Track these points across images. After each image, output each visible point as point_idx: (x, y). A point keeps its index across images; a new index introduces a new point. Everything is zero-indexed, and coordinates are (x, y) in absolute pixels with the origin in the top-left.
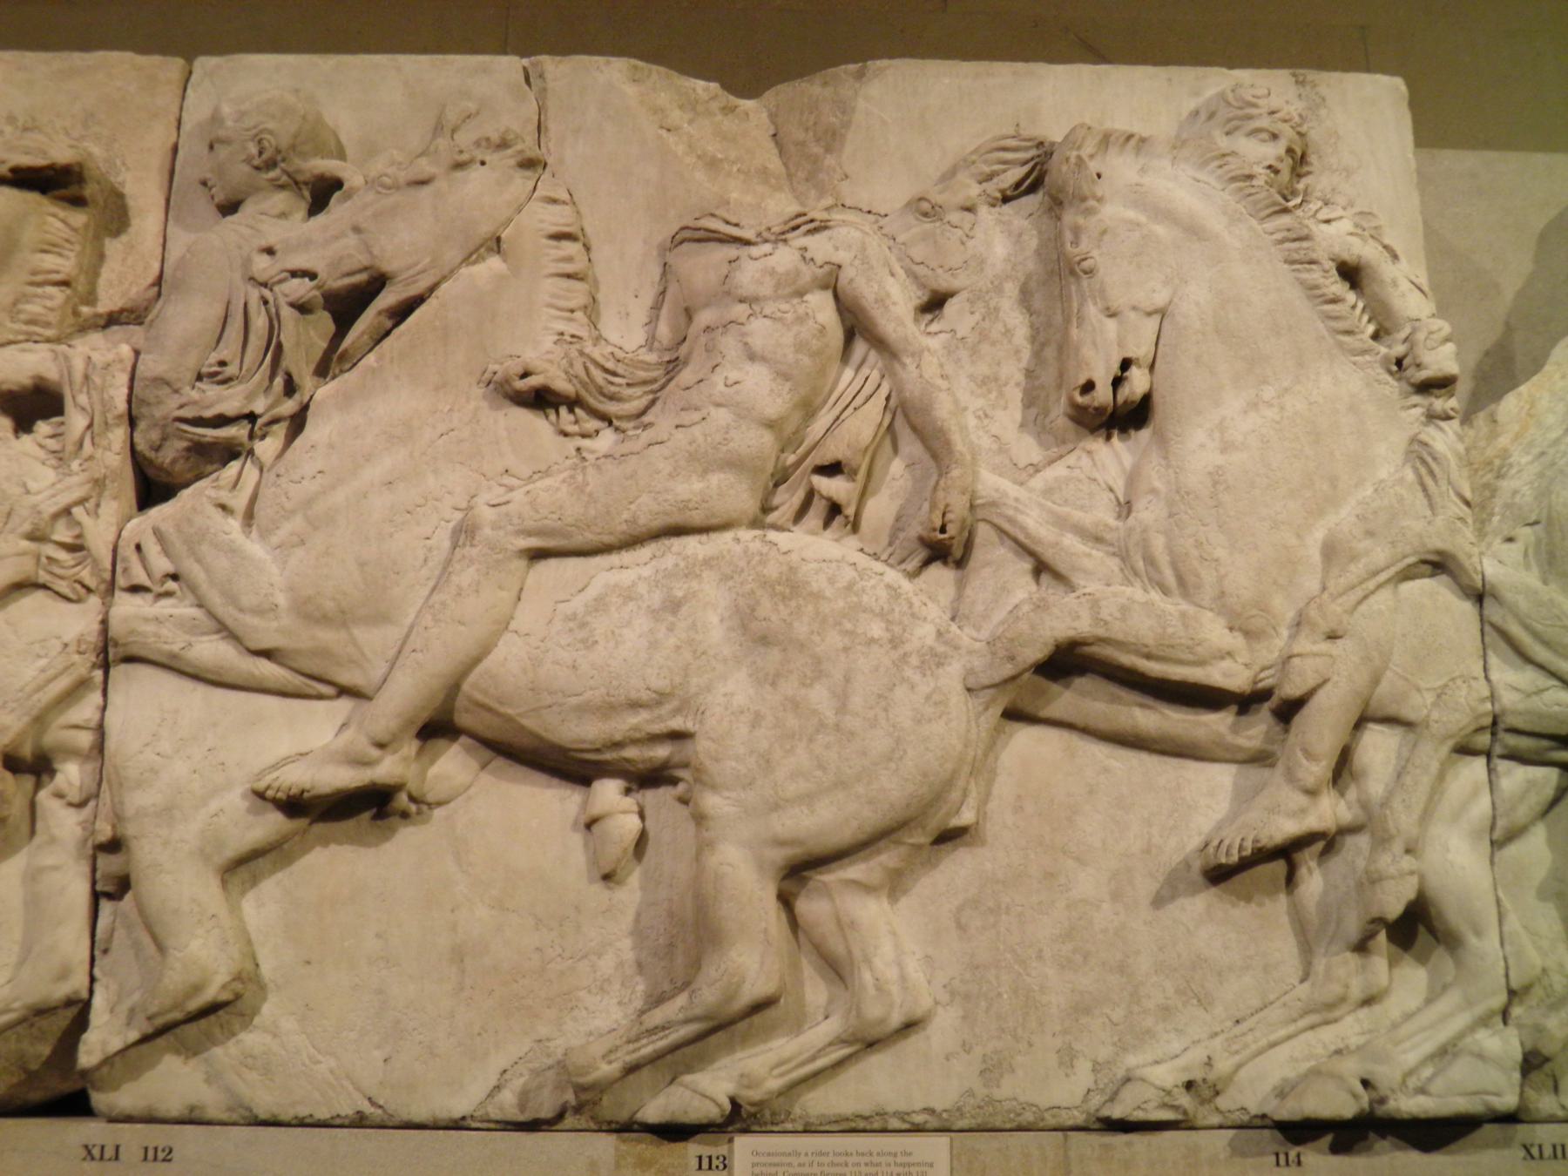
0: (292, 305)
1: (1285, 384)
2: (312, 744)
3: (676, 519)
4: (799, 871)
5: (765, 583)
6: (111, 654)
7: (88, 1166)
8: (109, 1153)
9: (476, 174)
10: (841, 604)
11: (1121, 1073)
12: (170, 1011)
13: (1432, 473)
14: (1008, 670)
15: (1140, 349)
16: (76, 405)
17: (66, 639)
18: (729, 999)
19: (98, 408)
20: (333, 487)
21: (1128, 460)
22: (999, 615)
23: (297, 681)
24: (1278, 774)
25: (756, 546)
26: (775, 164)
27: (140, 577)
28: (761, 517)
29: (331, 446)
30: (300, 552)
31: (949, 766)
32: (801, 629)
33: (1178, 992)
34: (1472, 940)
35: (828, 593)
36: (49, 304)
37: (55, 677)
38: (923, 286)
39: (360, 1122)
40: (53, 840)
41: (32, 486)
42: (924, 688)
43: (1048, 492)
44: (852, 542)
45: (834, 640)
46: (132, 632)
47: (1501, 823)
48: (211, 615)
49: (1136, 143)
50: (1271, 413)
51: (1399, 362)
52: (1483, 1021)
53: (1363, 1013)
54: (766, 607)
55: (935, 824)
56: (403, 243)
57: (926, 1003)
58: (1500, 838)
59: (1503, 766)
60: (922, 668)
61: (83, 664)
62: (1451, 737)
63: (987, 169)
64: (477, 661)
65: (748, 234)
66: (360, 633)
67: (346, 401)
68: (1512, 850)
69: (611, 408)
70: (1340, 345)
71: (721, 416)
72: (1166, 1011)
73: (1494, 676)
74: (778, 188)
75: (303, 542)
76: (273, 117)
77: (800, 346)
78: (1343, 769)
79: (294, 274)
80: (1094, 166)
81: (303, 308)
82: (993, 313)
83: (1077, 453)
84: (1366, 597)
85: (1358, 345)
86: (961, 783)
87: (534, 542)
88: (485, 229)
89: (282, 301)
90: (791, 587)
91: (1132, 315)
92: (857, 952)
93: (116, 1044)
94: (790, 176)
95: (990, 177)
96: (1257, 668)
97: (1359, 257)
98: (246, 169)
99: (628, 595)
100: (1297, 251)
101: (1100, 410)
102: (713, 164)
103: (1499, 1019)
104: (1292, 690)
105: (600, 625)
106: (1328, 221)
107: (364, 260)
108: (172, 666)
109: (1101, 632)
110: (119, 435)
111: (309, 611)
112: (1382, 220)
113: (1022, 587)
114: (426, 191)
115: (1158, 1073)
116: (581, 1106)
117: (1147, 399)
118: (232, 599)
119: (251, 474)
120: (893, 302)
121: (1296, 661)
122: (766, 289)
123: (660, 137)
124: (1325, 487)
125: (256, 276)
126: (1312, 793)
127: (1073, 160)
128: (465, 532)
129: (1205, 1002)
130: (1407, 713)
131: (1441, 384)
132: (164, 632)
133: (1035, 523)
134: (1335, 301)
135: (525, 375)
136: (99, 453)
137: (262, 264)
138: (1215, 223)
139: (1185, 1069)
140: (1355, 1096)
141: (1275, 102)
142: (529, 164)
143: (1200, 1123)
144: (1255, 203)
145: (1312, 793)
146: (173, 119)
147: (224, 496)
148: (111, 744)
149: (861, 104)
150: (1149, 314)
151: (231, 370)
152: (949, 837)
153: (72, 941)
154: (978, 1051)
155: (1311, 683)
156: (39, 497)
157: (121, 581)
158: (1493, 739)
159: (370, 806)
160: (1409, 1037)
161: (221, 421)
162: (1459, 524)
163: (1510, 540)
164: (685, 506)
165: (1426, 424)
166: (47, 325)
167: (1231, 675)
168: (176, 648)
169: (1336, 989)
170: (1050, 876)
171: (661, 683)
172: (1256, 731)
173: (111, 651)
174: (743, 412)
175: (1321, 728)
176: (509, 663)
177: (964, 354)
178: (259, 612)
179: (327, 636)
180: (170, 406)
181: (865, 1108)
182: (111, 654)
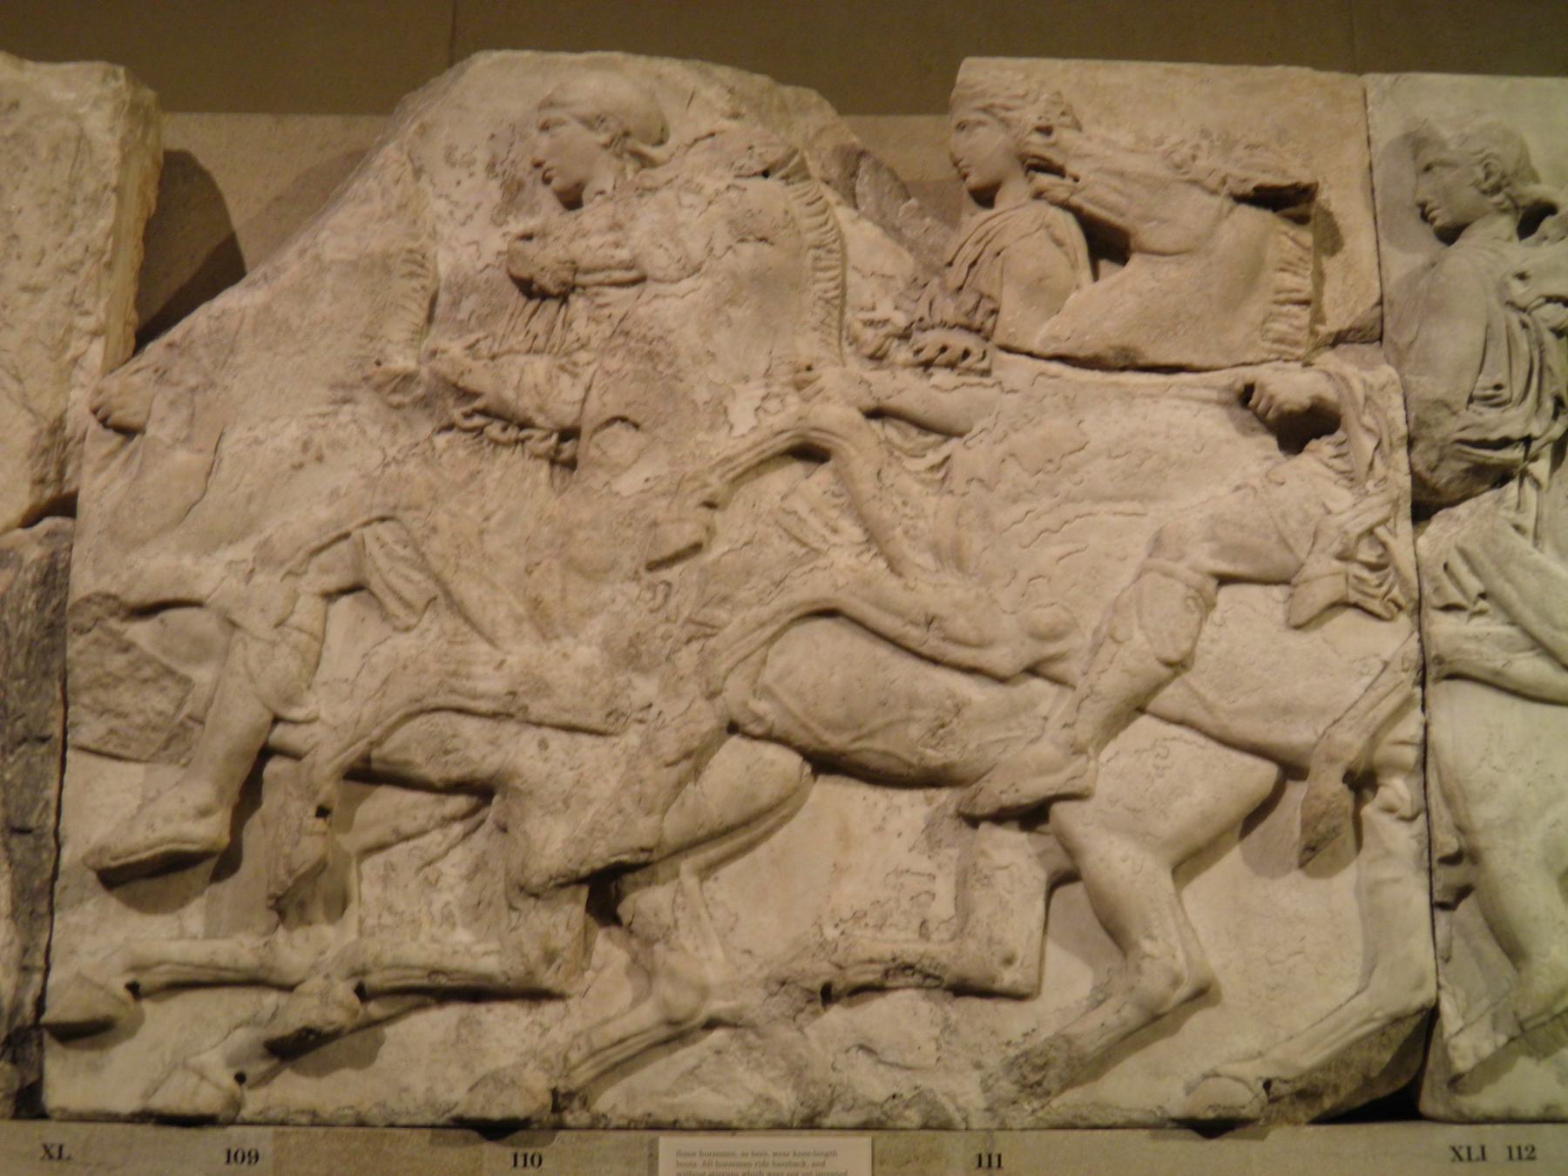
6: (1433, 670)
8: (1476, 1153)
12: (1541, 1014)
17: (1386, 656)
19: (1384, 428)
27: (1456, 597)
36: (1296, 323)
40: (1388, 854)
46: (1457, 650)
48: (1527, 632)
89: (1543, 326)
93: (1487, 1049)
98: (1474, 192)
108: (1497, 684)
118: (1546, 617)
132: (1484, 649)
136: (1391, 474)
137: (1518, 290)
146: (1364, 136)
151: (1505, 393)
153: (1421, 951)
156: (1343, 518)
161: (1505, 443)
166: (1296, 344)
168: (1499, 664)
173: (1433, 671)
180: (1450, 428)
182: (1433, 670)
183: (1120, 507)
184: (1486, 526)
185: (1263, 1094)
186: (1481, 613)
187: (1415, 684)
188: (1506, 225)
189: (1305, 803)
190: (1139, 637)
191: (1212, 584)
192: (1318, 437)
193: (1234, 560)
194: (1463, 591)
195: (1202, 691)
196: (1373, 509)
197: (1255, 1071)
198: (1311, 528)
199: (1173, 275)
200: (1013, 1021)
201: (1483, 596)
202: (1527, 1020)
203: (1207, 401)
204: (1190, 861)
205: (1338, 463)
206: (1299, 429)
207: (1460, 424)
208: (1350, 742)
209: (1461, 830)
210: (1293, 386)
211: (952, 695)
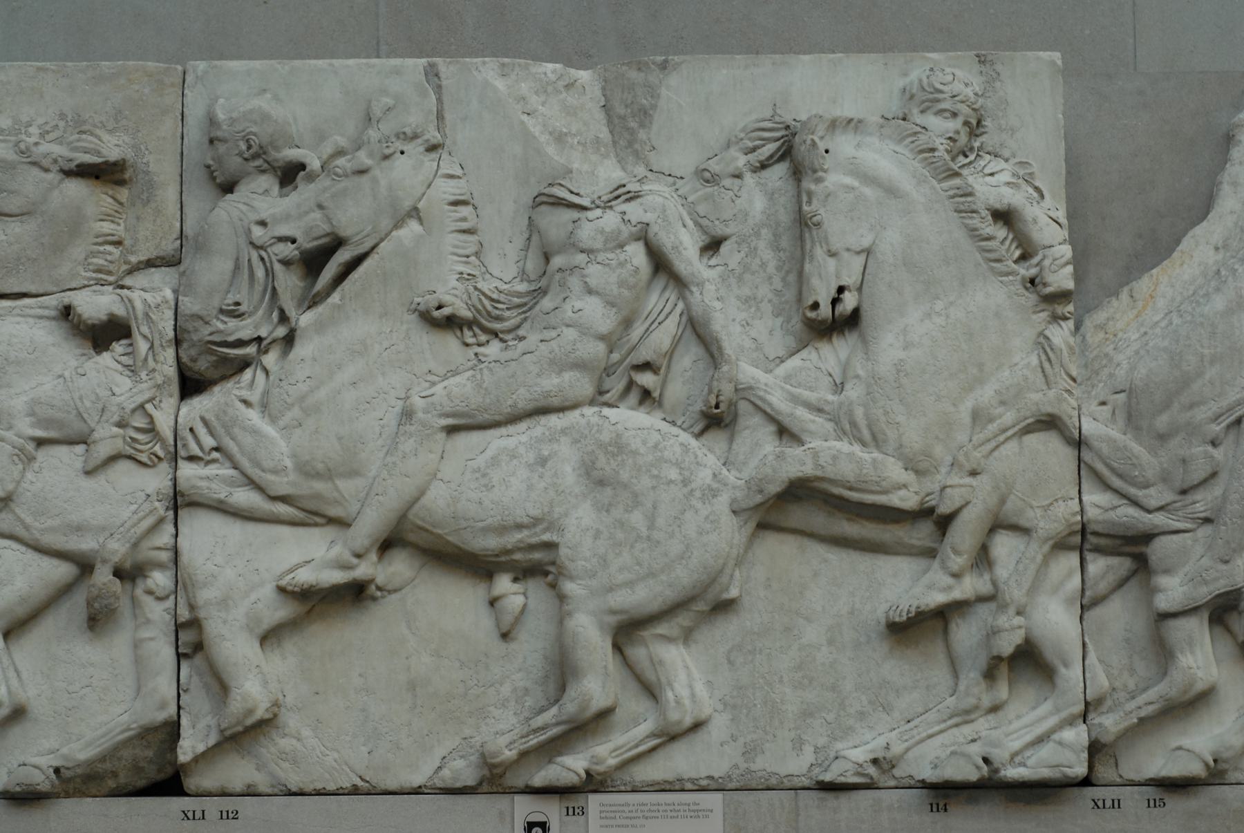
0: (280, 261)
1: (952, 299)
2: (314, 557)
3: (542, 403)
4: (627, 631)
5: (602, 446)
6: (180, 501)
7: (186, 823)
9: (400, 161)
10: (651, 457)
11: (832, 755)
12: (235, 726)
13: (1049, 360)
14: (759, 499)
16: (141, 334)
17: (148, 492)
19: (157, 336)
20: (318, 388)
21: (843, 355)
22: (754, 463)
24: (936, 564)
26: (604, 134)
27: (196, 451)
28: (599, 397)
30: (298, 431)
31: (721, 561)
32: (625, 476)
33: (870, 702)
34: (1062, 670)
35: (642, 451)
36: (109, 258)
37: (144, 517)
38: (706, 233)
39: (355, 791)
40: (148, 621)
41: (116, 390)
42: (704, 512)
43: (787, 378)
44: (659, 414)
45: (646, 482)
46: (193, 487)
47: (1088, 593)
49: (853, 125)
50: (940, 321)
51: (1032, 281)
52: (1070, 722)
53: (991, 717)
54: (602, 461)
55: (711, 596)
56: (353, 216)
57: (706, 711)
58: (1087, 604)
59: (1089, 556)
60: (703, 498)
61: (160, 508)
62: (1051, 538)
63: (750, 144)
64: (417, 499)
65: (585, 202)
66: (342, 484)
67: (320, 327)
69: (497, 326)
70: (992, 269)
71: (570, 334)
72: (862, 715)
73: (1085, 498)
74: (605, 156)
75: (300, 425)
76: (256, 123)
77: (622, 284)
78: (983, 558)
79: (281, 239)
80: (822, 146)
81: (286, 263)
82: (753, 252)
83: (809, 348)
84: (997, 447)
85: (1004, 269)
86: (728, 571)
87: (450, 421)
88: (407, 204)
89: (274, 258)
90: (617, 447)
91: (846, 255)
92: (663, 680)
93: (201, 748)
94: (614, 142)
95: (754, 150)
96: (923, 494)
97: (1009, 205)
98: (239, 160)
99: (513, 455)
100: (963, 203)
101: (823, 322)
102: (560, 138)
103: (1081, 720)
104: (944, 509)
106: (992, 174)
107: (326, 228)
109: (819, 473)
110: (170, 353)
111: (306, 470)
112: (1035, 168)
113: (769, 445)
114: (364, 179)
115: (855, 754)
116: (493, 780)
118: (257, 464)
119: (260, 375)
121: (948, 490)
122: (598, 245)
123: (523, 122)
124: (975, 371)
125: (255, 241)
126: (956, 576)
127: (809, 142)
128: (407, 414)
129: (887, 709)
130: (1023, 522)
131: (1063, 296)
132: (213, 486)
133: (778, 401)
134: (989, 239)
135: (440, 307)
136: (158, 367)
138: (906, 184)
139: (871, 751)
140: (978, 768)
141: (957, 87)
142: (432, 148)
143: (881, 785)
144: (936, 169)
145: (956, 576)
147: (245, 394)
148: (184, 558)
149: (664, 92)
150: (858, 253)
152: (724, 607)
154: (742, 740)
155: (957, 505)
156: (122, 398)
157: (182, 453)
158: (1083, 539)
159: (356, 593)
160: (1016, 731)
161: (240, 343)
162: (1066, 395)
163: (1103, 403)
164: (547, 395)
165: (1050, 323)
166: (109, 273)
167: (906, 500)
168: (222, 496)
169: (972, 701)
170: (787, 629)
171: (535, 512)
172: (921, 534)
173: (179, 500)
174: (585, 331)
175: (964, 534)
176: (437, 500)
177: (733, 281)
178: (275, 472)
179: (319, 486)
180: (205, 331)
181: (670, 776)
182: (180, 501)
184: (222, 401)
185: (53, 776)
186: (214, 461)
187: (167, 509)
188: (267, 182)
189: (94, 589)
191: (30, 447)
192: (119, 340)
193: (47, 429)
194: (201, 448)
195: (23, 516)
196: (144, 391)
197: (47, 762)
198: (100, 406)
199: (17, 230)
201: (217, 449)
202: (225, 730)
203: (41, 317)
205: (124, 359)
206: (105, 334)
207: (209, 329)
208: (117, 549)
209: (192, 607)
210: (96, 304)
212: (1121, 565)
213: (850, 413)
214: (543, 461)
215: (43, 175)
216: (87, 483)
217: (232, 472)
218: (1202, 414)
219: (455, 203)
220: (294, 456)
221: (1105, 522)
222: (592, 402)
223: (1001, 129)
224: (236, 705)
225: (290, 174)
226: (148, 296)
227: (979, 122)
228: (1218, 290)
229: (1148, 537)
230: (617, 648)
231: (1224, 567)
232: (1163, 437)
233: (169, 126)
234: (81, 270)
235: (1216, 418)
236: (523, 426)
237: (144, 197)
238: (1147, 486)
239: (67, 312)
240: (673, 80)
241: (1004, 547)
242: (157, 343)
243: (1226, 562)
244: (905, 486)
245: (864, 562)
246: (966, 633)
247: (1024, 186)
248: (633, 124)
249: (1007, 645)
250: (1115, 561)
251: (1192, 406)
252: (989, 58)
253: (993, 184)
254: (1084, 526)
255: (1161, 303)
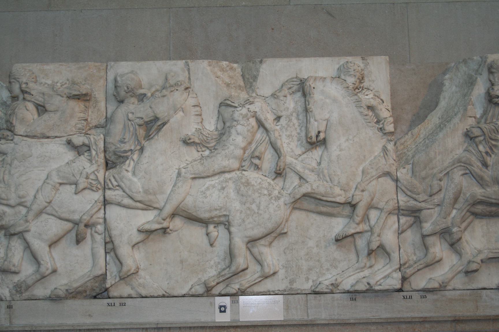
3: (223, 170)
5: (242, 183)
6: (106, 202)
7: (109, 307)
8: (113, 304)
10: (258, 187)
11: (318, 283)
13: (387, 154)
15: (322, 129)
17: (96, 200)
18: (237, 269)
21: (320, 153)
23: (145, 207)
25: (240, 175)
26: (242, 84)
28: (241, 168)
29: (149, 157)
31: (281, 220)
32: (250, 193)
34: (392, 254)
35: (255, 185)
38: (275, 115)
39: (163, 296)
41: (85, 167)
42: (276, 204)
43: (302, 161)
44: (261, 173)
45: (257, 195)
47: (401, 229)
50: (351, 142)
51: (381, 128)
52: (395, 271)
53: (369, 270)
55: (278, 231)
57: (277, 269)
58: (400, 232)
59: (400, 217)
60: (275, 200)
61: (100, 205)
63: (289, 86)
65: (236, 105)
68: (403, 234)
70: (368, 125)
71: (232, 147)
72: (328, 270)
74: (243, 91)
77: (248, 131)
78: (366, 218)
80: (313, 86)
81: (140, 125)
82: (290, 120)
86: (283, 223)
87: (193, 176)
92: (263, 259)
94: (246, 87)
99: (214, 187)
103: (398, 270)
104: (353, 203)
105: (208, 193)
107: (153, 114)
108: (119, 204)
109: (313, 191)
110: (102, 155)
111: (146, 192)
114: (165, 98)
117: (324, 139)
118: (130, 190)
120: (269, 118)
123: (216, 80)
129: (336, 267)
133: (299, 168)
136: (99, 160)
137: (130, 116)
140: (366, 286)
146: (105, 78)
149: (261, 70)
151: (126, 140)
154: (289, 278)
155: (358, 201)
157: (107, 187)
158: (399, 211)
163: (404, 168)
164: (225, 167)
168: (120, 201)
170: (303, 242)
171: (221, 205)
175: (360, 211)
176: (189, 201)
177: (284, 130)
178: (136, 193)
181: (265, 290)
182: (106, 202)
183: (39, 169)
189: (79, 231)
190: (41, 197)
191: (58, 185)
194: (113, 186)
196: (94, 167)
197: (64, 288)
200: (16, 279)
201: (118, 186)
203: (61, 144)
204: (52, 244)
210: (78, 140)
211: (3, 211)
212: (411, 219)
213: (323, 172)
214: (223, 188)
215: (61, 98)
216: (75, 197)
217: (124, 193)
218: (435, 171)
219: (194, 106)
220: (143, 188)
221: (405, 206)
222: (238, 170)
223: (370, 81)
224: (125, 269)
225: (142, 98)
226: (95, 137)
227: (363, 78)
228: (440, 131)
229: (420, 210)
230: (248, 249)
231: (444, 220)
232: (424, 179)
233: (102, 82)
234: (74, 129)
235: (441, 172)
236: (217, 177)
237: (94, 105)
238: (419, 194)
239: (69, 142)
240: (264, 66)
241: (374, 215)
242: (99, 151)
243: (445, 218)
244: (341, 195)
245: (328, 220)
246: (361, 243)
247: (377, 99)
248: (251, 81)
249: (374, 246)
250: (409, 218)
251: (433, 168)
252: (366, 58)
253: (368, 98)
254: (398, 207)
255: (422, 136)
